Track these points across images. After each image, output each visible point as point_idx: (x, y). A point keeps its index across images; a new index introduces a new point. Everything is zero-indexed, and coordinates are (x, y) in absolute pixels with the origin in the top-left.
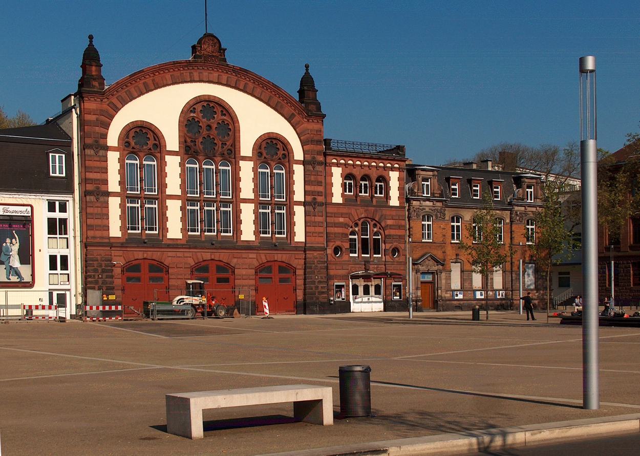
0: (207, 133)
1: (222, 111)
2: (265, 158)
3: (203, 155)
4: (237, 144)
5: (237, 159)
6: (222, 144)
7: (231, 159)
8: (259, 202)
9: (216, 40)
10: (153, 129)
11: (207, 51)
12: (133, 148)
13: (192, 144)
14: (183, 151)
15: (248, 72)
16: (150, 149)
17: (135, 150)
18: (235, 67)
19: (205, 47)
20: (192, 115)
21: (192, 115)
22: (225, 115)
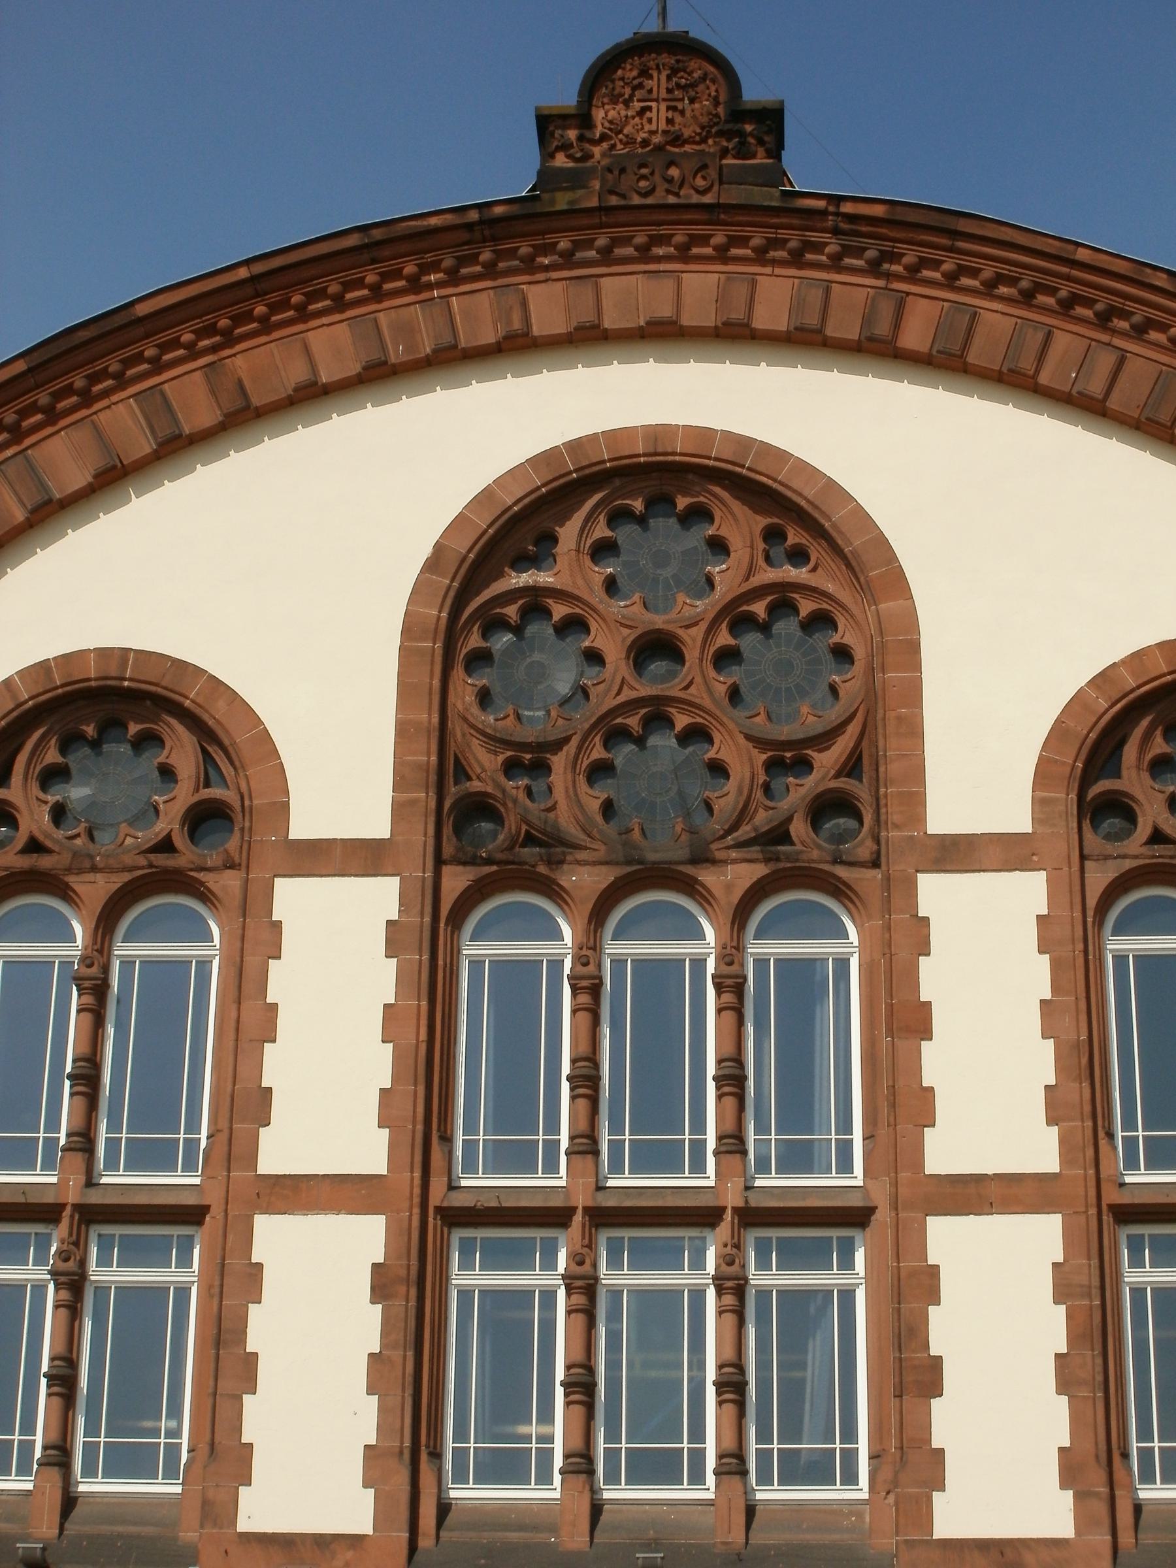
0: (645, 690)
1: (773, 535)
2: (1158, 837)
3: (602, 851)
4: (892, 745)
5: (897, 866)
6: (770, 765)
7: (842, 872)
8: (1112, 1196)
9: (698, 68)
10: (192, 696)
11: (630, 141)
12: (34, 846)
13: (516, 786)
14: (420, 836)
15: (964, 226)
16: (166, 846)
17: (45, 862)
18: (847, 208)
19: (616, 112)
20: (524, 579)
21: (524, 579)
22: (798, 556)
